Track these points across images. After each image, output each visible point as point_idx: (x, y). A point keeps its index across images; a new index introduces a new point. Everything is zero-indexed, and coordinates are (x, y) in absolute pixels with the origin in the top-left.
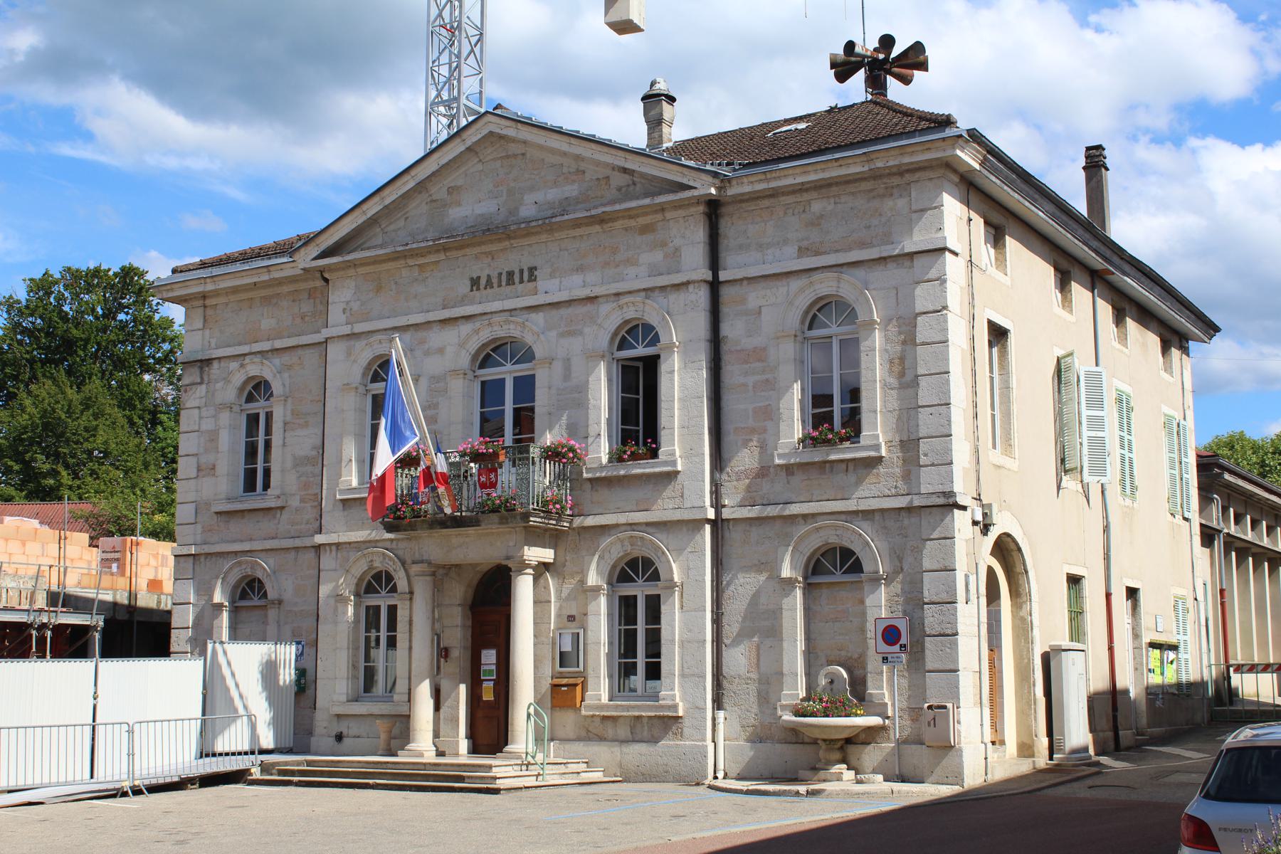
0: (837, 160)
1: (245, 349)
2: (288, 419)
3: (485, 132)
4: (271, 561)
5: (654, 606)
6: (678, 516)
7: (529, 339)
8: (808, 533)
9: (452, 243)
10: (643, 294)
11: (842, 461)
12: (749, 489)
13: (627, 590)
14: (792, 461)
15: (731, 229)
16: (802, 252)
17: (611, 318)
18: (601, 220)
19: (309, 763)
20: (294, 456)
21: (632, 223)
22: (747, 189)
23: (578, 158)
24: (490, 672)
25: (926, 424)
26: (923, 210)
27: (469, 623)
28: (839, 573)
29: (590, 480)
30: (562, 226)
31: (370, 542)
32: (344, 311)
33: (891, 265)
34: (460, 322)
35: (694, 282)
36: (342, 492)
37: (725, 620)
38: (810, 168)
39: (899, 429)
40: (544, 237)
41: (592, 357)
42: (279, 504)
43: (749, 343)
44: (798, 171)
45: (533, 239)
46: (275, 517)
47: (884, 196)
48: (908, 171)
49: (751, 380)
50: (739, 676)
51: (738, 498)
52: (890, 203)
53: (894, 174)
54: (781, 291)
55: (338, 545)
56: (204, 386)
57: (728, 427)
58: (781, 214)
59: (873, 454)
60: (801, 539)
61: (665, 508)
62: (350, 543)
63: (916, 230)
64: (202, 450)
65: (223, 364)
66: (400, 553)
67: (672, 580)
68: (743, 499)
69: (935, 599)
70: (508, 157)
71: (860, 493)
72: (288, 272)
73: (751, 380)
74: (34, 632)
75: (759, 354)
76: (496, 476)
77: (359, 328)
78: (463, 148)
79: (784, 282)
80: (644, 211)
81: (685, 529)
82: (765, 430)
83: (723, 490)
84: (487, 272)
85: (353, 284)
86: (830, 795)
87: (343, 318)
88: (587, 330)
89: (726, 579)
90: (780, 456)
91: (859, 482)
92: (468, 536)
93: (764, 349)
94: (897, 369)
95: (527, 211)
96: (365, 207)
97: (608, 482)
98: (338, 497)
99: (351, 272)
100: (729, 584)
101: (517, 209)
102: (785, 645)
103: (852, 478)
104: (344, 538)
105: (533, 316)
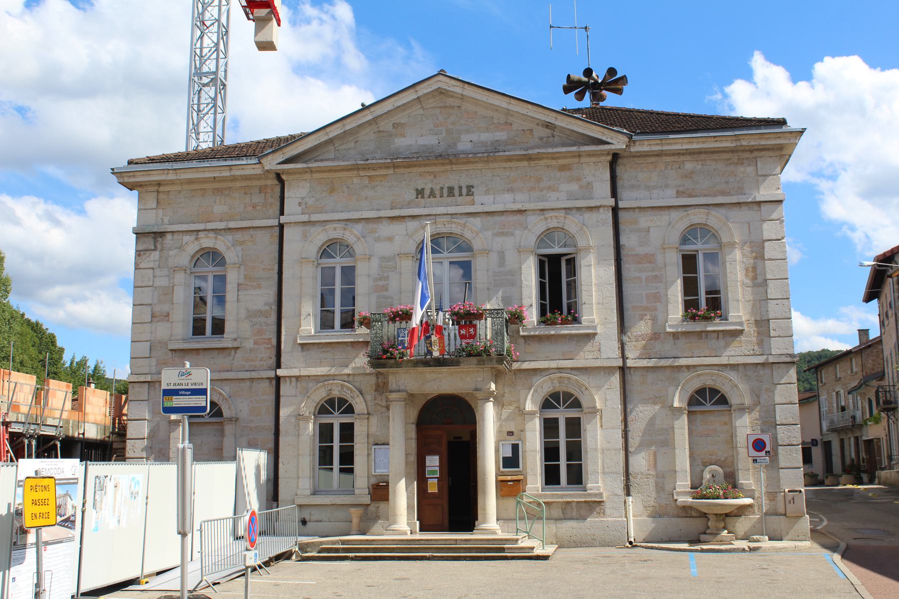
0: (715, 137)
1: (201, 226)
2: (241, 281)
3: (435, 87)
4: (227, 388)
5: (574, 427)
6: (598, 363)
7: (468, 235)
8: (693, 377)
9: (403, 162)
10: (564, 211)
11: (714, 331)
12: (645, 347)
13: (551, 414)
14: (680, 330)
15: (625, 173)
16: (679, 194)
17: (537, 225)
18: (529, 158)
19: (343, 542)
20: (248, 310)
21: (554, 162)
22: (645, 148)
23: (508, 112)
24: (434, 472)
25: (773, 309)
26: (766, 176)
27: (413, 434)
28: (708, 405)
29: (524, 337)
30: (496, 160)
31: (328, 376)
32: (300, 204)
33: (744, 208)
34: (407, 220)
35: (604, 206)
36: (302, 338)
37: (630, 435)
38: (694, 140)
39: (753, 313)
40: (480, 166)
41: (520, 250)
42: (235, 345)
43: (641, 250)
44: (685, 141)
45: (470, 166)
46: (229, 355)
47: (737, 164)
48: (757, 150)
49: (644, 275)
50: (642, 473)
51: (637, 354)
52: (742, 169)
53: (747, 151)
54: (664, 218)
55: (297, 378)
56: (157, 253)
57: (627, 305)
58: (663, 168)
59: (738, 328)
60: (687, 381)
61: (585, 357)
62: (309, 376)
63: (762, 188)
64: (155, 301)
65: (176, 236)
66: (357, 384)
67: (595, 407)
68: (641, 354)
69: (784, 422)
70: (445, 107)
71: (728, 353)
72: (249, 171)
73: (644, 275)
74: (26, 441)
75: (649, 258)
76: (475, 330)
77: (314, 218)
78: (416, 97)
79: (667, 212)
80: (564, 156)
81: (602, 373)
82: (656, 309)
83: (626, 347)
84: (430, 186)
85: (308, 185)
86: (765, 551)
87: (299, 209)
88: (517, 233)
89: (629, 407)
90: (670, 326)
91: (727, 346)
92: (440, 373)
93: (653, 255)
94: (751, 274)
95: (464, 144)
96: (328, 130)
97: (539, 339)
98: (299, 342)
99: (308, 176)
100: (631, 411)
101: (455, 144)
102: (677, 451)
103: (722, 343)
104: (304, 372)
105: (471, 219)
